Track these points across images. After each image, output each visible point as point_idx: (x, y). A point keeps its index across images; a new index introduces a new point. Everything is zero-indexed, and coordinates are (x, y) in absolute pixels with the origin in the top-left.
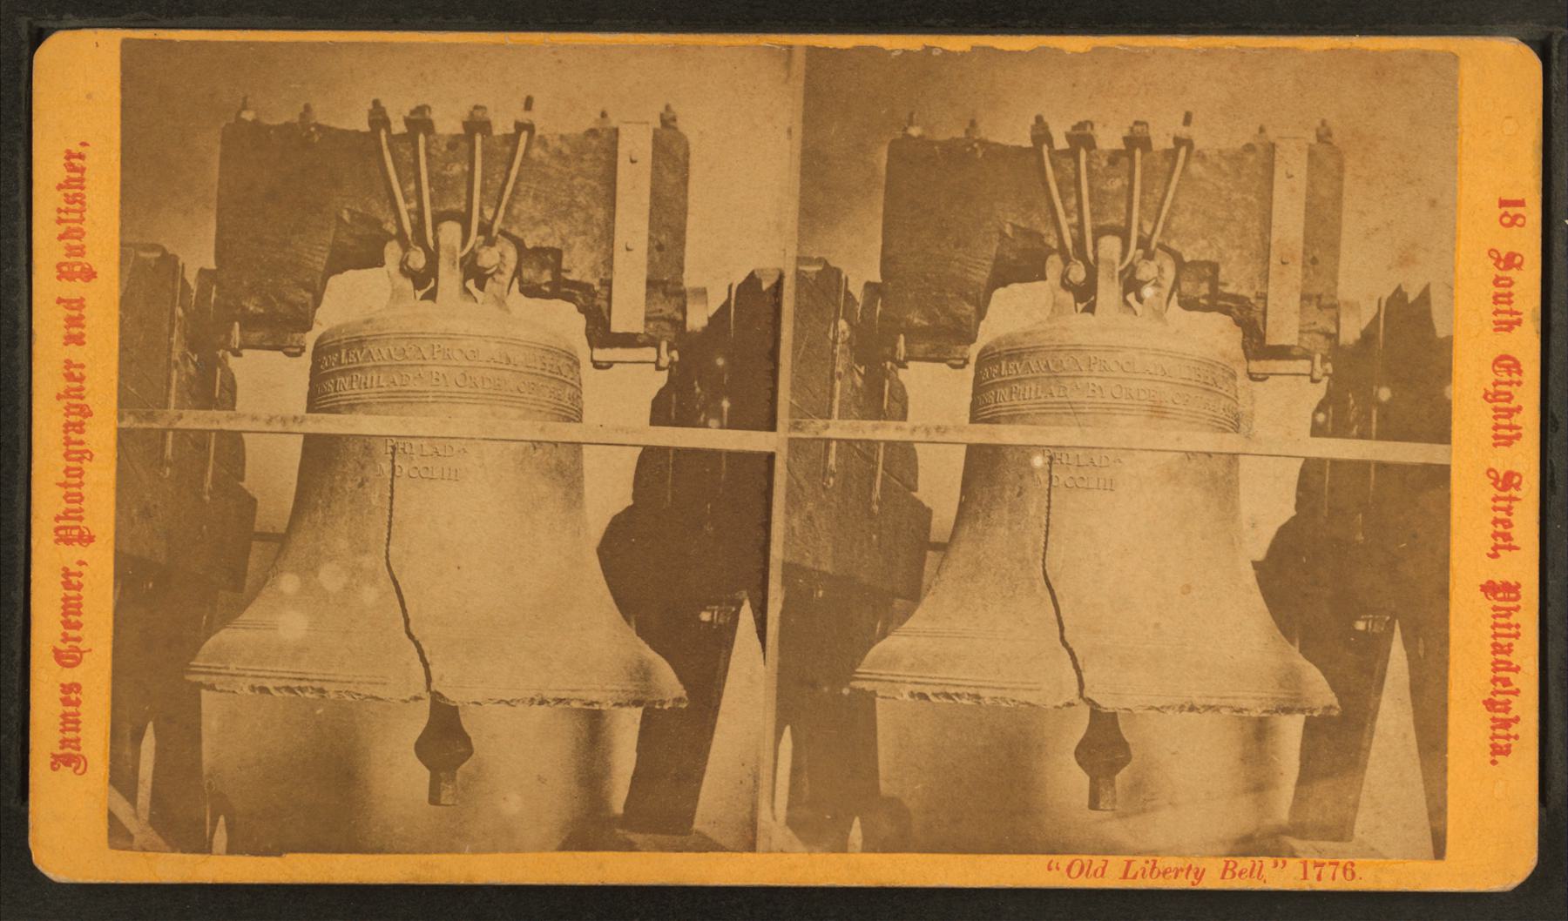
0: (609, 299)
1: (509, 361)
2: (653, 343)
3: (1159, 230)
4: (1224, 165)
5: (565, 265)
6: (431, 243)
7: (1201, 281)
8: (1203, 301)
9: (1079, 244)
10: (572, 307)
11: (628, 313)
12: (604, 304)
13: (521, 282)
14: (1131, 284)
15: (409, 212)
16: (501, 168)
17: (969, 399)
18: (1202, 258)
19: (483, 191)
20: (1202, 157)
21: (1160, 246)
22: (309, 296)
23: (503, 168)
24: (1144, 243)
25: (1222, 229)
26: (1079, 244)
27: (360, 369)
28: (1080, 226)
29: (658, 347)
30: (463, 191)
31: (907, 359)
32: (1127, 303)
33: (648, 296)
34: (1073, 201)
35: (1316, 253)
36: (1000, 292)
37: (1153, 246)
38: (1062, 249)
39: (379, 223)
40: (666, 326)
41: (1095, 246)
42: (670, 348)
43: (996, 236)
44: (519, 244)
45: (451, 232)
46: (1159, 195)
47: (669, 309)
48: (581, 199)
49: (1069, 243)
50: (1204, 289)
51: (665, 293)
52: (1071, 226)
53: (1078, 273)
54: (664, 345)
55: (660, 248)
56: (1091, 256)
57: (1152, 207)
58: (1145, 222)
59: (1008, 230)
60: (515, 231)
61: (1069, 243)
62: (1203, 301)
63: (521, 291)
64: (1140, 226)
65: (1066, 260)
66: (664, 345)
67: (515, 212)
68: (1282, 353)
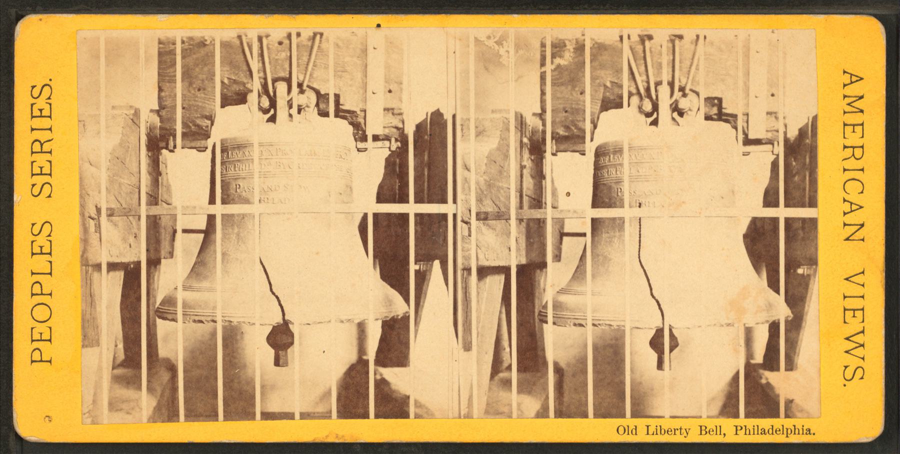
0: (365, 118)
1: (315, 154)
2: (387, 138)
3: (690, 82)
4: (723, 46)
5: (341, 102)
6: (272, 94)
7: (713, 105)
8: (715, 117)
9: (648, 89)
10: (346, 122)
11: (375, 124)
12: (362, 121)
13: (319, 110)
14: (676, 109)
15: (260, 78)
16: (306, 54)
17: (593, 172)
18: (714, 96)
19: (298, 66)
20: (712, 44)
21: (691, 90)
22: (209, 122)
23: (308, 54)
24: (682, 89)
25: (723, 80)
26: (648, 89)
27: (239, 161)
28: (648, 82)
29: (390, 140)
30: (287, 66)
31: (557, 151)
32: (673, 119)
33: (384, 116)
34: (643, 68)
35: (774, 91)
36: (605, 113)
37: (687, 91)
38: (639, 93)
39: (244, 84)
40: (395, 130)
41: (656, 91)
42: (396, 140)
43: (602, 89)
44: (317, 92)
45: (282, 87)
46: (689, 64)
47: (396, 122)
48: (348, 68)
49: (642, 91)
50: (715, 110)
51: (393, 114)
52: (642, 81)
53: (648, 107)
54: (393, 140)
55: (390, 91)
56: (654, 97)
57: (685, 70)
58: (682, 78)
59: (608, 84)
60: (315, 86)
61: (642, 91)
62: (715, 117)
63: (319, 114)
64: (680, 81)
65: (641, 99)
66: (393, 140)
67: (315, 76)
68: (758, 142)
